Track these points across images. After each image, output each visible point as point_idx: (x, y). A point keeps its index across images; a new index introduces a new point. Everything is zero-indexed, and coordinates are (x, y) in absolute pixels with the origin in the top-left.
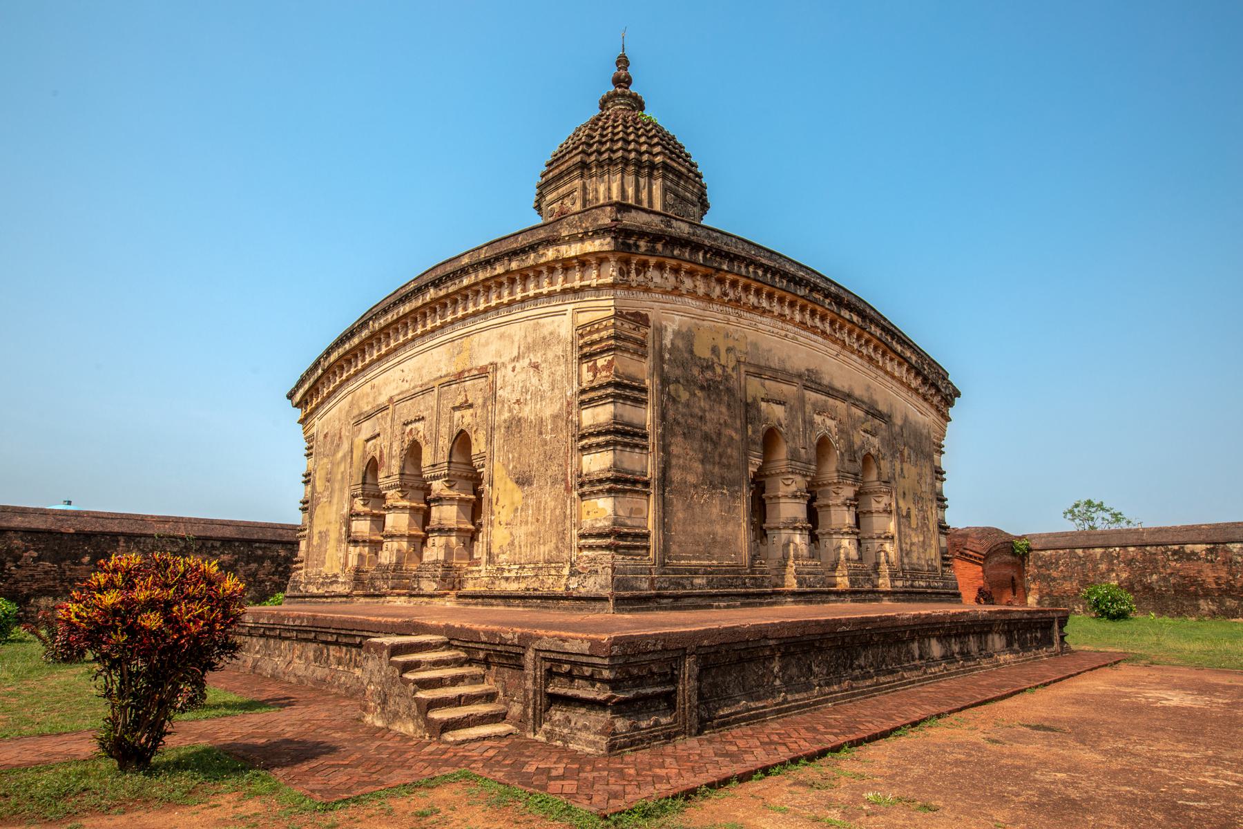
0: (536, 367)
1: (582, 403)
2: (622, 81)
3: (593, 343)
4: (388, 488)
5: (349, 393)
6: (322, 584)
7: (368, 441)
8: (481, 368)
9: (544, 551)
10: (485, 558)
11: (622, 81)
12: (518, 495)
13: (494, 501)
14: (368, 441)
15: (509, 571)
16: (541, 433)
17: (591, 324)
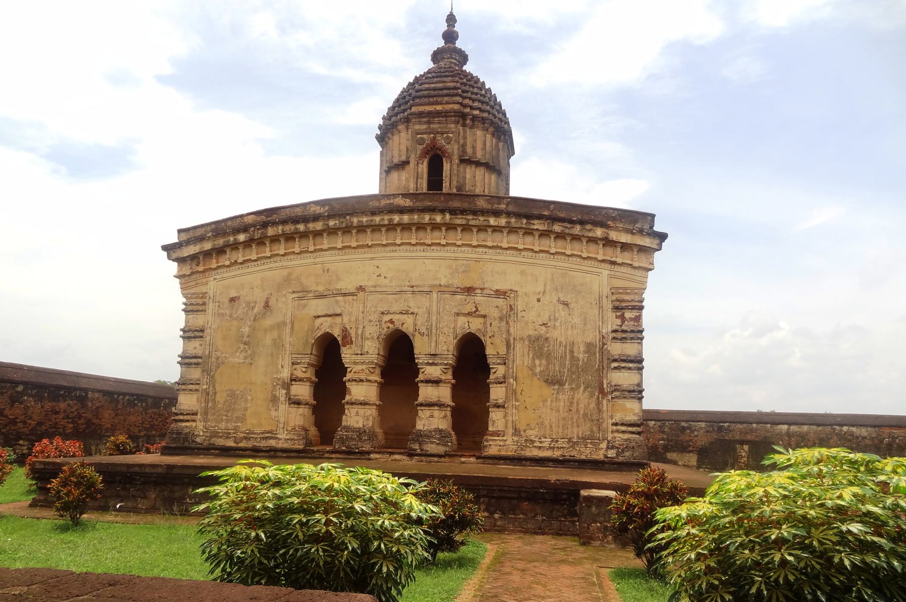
0: (566, 304)
1: (614, 338)
2: (450, 36)
3: (623, 301)
4: (355, 363)
5: (283, 268)
6: (245, 438)
7: (319, 317)
8: (497, 291)
9: (575, 433)
10: (510, 431)
11: (450, 36)
12: (547, 391)
13: (519, 391)
14: (319, 317)
15: (541, 442)
16: (572, 352)
17: (626, 288)
